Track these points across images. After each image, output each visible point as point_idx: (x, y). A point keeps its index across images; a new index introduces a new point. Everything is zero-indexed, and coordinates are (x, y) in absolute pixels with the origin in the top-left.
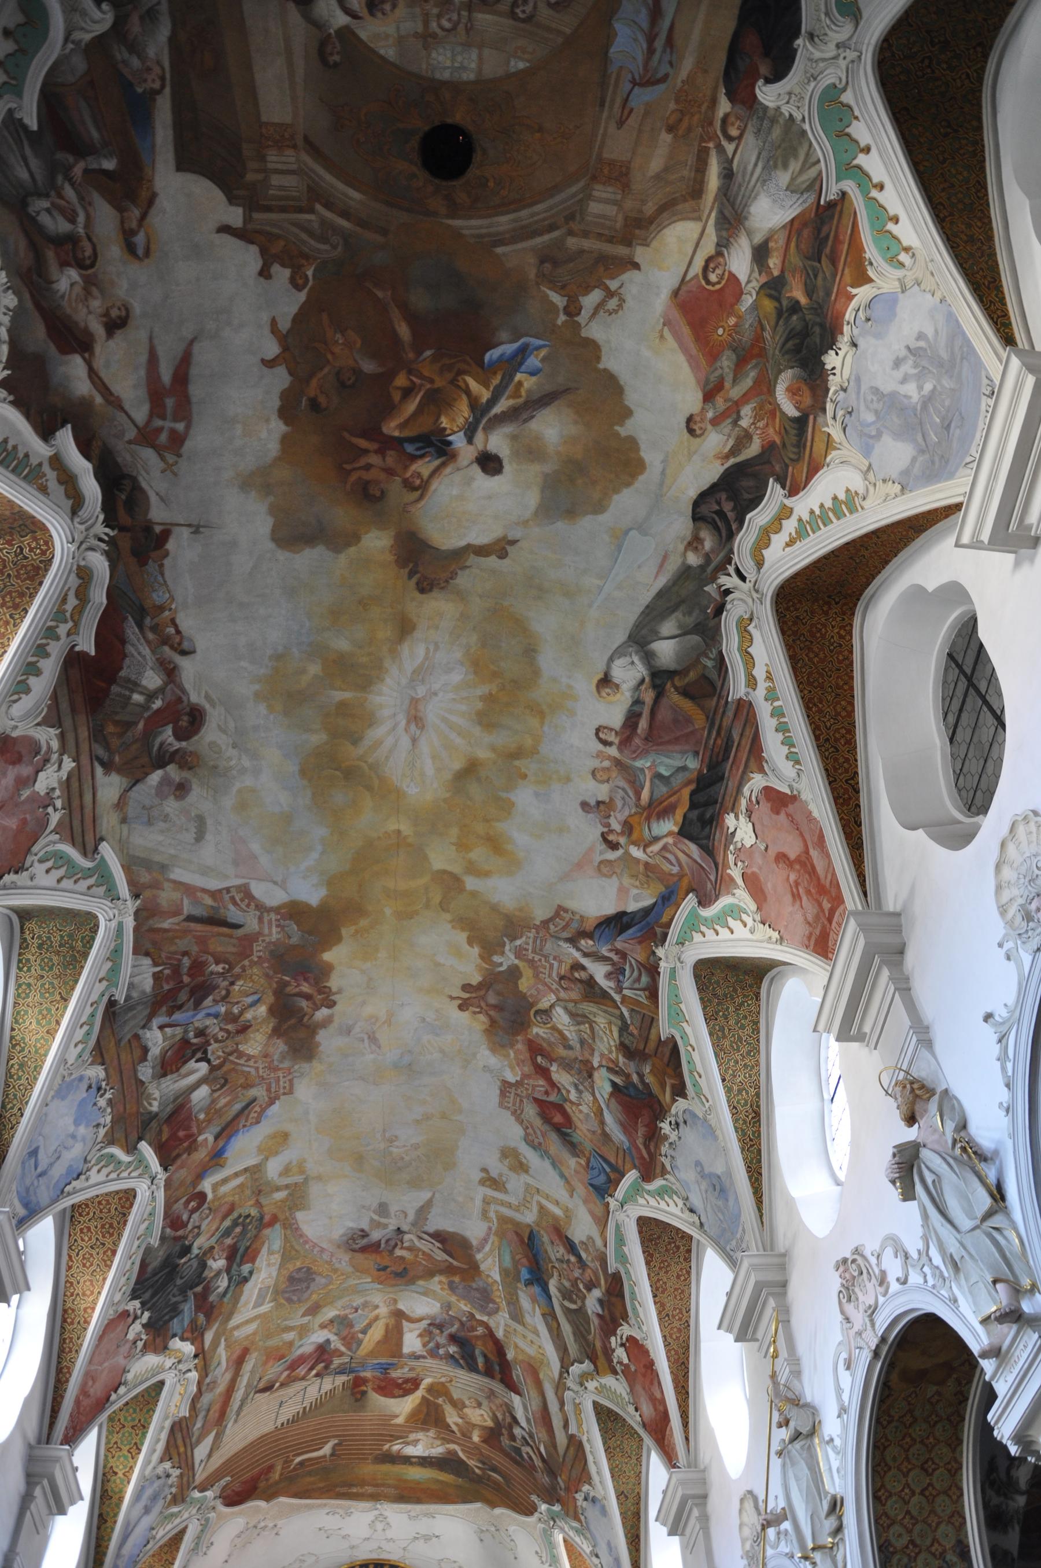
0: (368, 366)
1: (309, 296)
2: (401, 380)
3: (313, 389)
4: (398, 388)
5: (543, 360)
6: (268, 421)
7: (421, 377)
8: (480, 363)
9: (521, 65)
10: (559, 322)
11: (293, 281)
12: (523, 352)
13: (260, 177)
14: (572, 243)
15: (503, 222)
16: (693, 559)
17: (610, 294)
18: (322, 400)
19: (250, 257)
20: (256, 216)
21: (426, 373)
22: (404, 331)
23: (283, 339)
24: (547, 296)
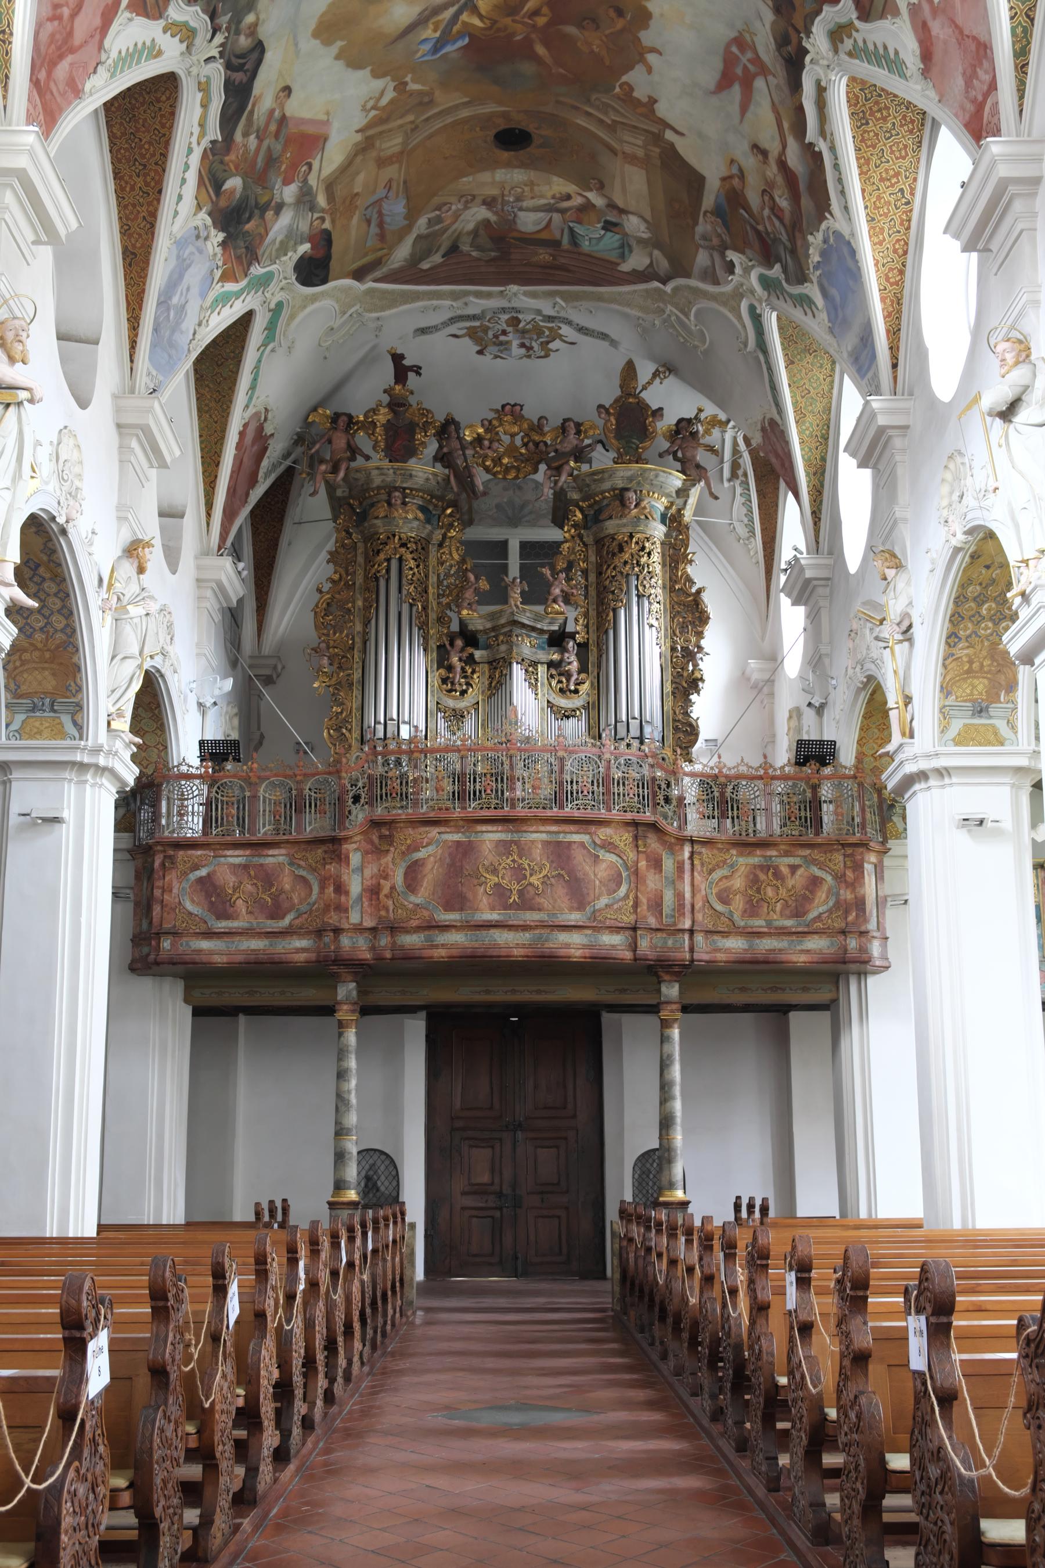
0: (571, 30)
1: (620, 78)
2: (541, 21)
3: (620, 24)
4: (544, 15)
5: (418, 50)
6: (662, 15)
7: (523, 23)
8: (471, 36)
9: (465, 179)
10: (410, 76)
11: (632, 89)
12: (436, 49)
13: (649, 147)
14: (410, 118)
15: (465, 113)
16: (250, 18)
17: (374, 108)
18: (612, 13)
19: (662, 110)
20: (656, 131)
21: (520, 25)
22: (540, 50)
23: (642, 60)
24: (423, 85)
